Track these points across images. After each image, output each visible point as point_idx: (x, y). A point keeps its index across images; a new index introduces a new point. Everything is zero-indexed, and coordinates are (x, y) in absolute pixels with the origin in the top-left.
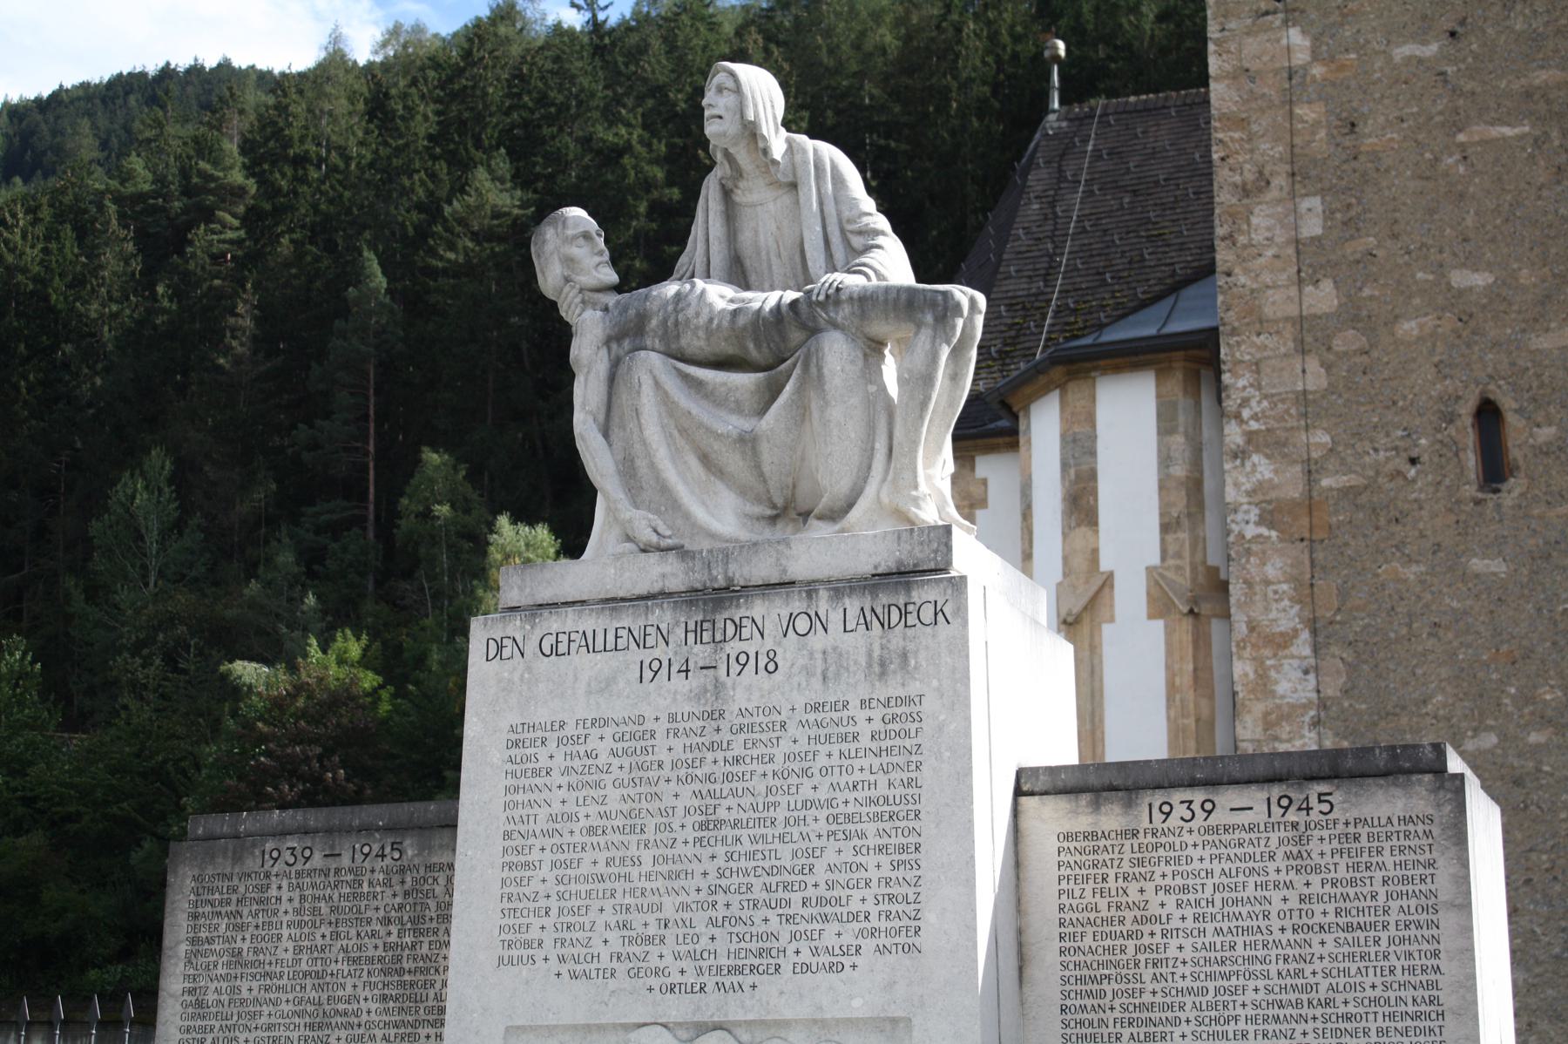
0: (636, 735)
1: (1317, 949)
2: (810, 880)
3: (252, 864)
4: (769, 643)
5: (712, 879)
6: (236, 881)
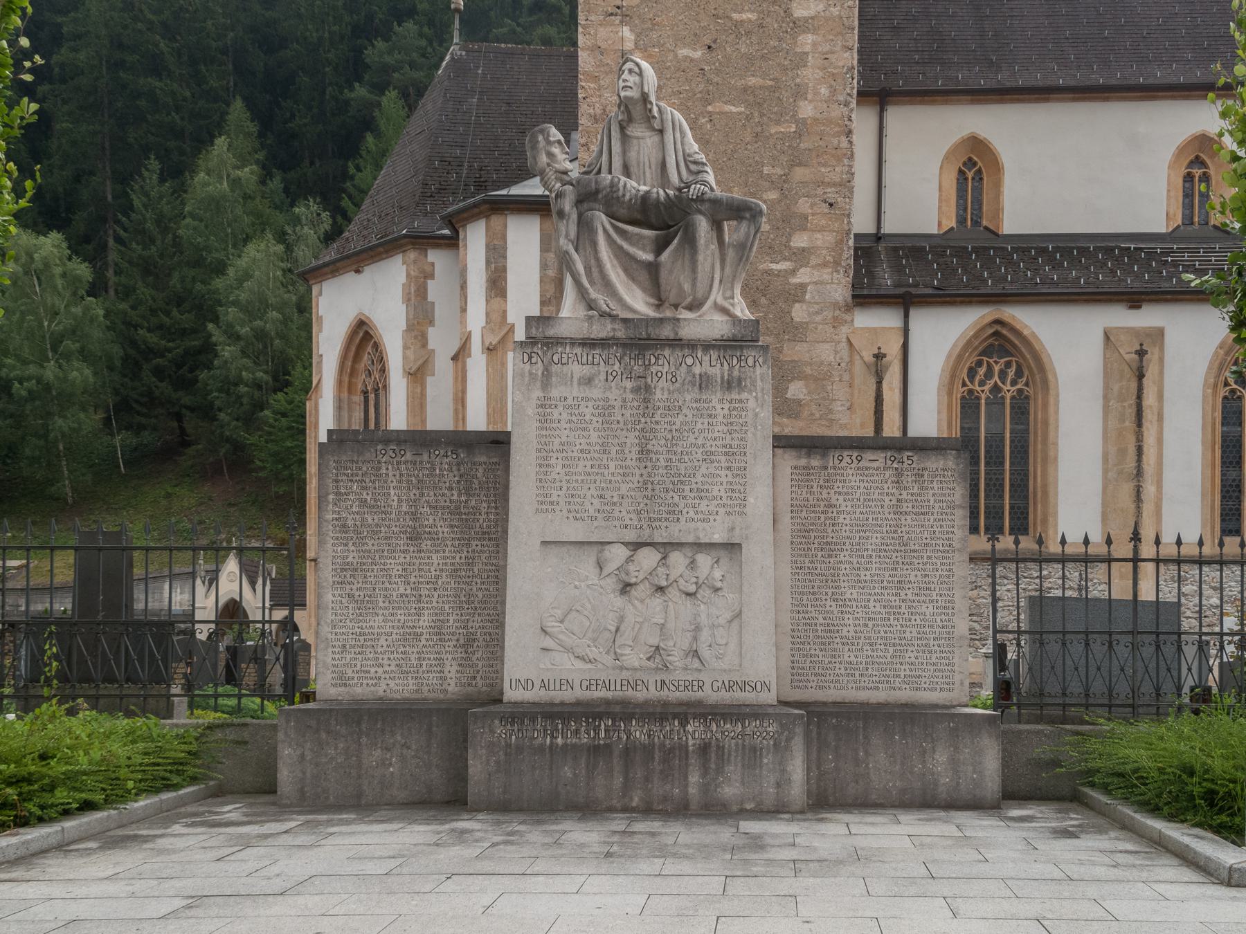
2: (694, 480)
3: (368, 456)
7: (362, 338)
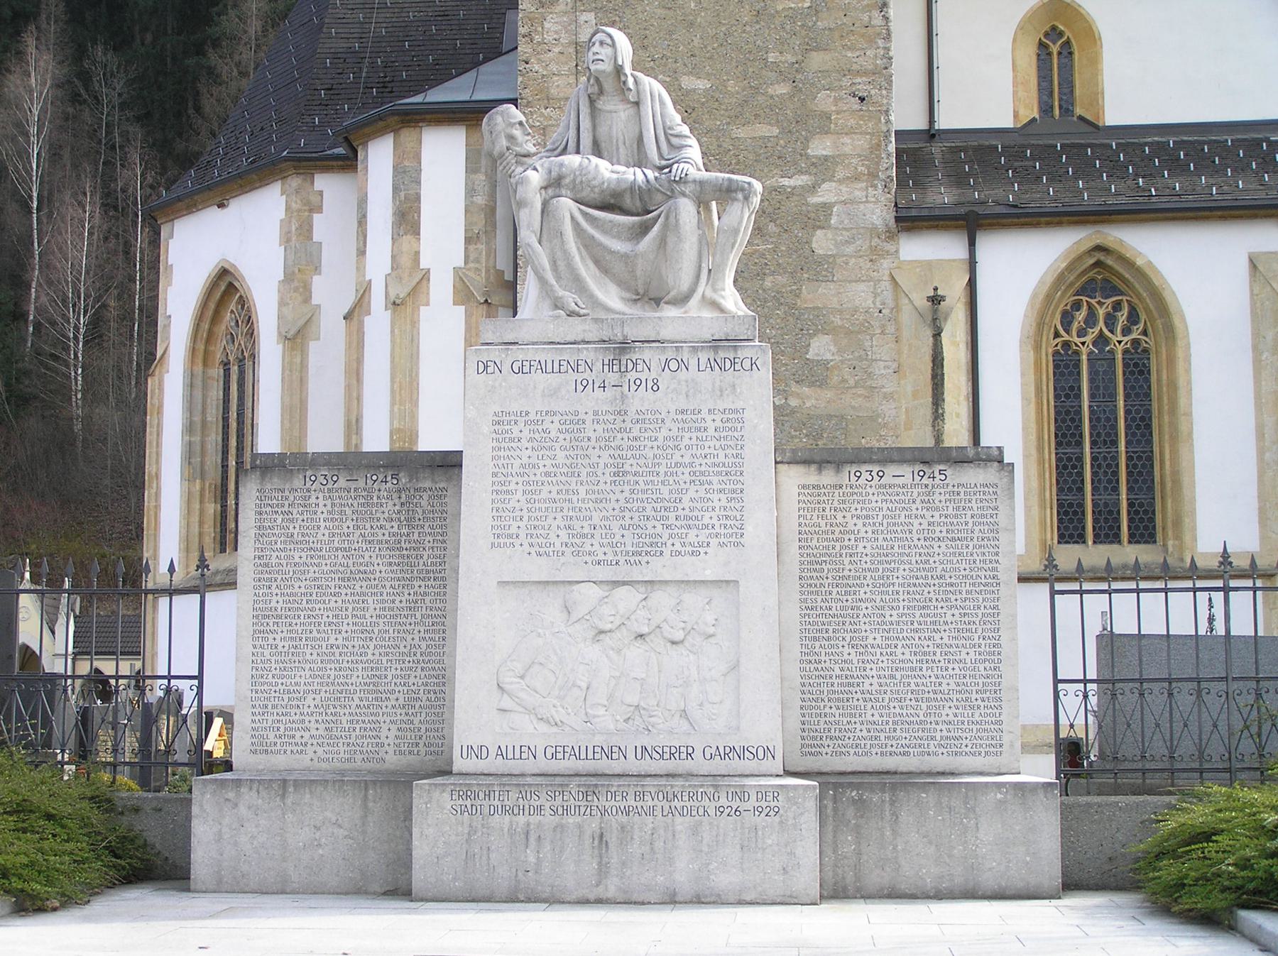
0: (573, 423)
1: (936, 550)
2: (680, 506)
4: (653, 375)
5: (622, 503)
6: (287, 493)
7: (225, 290)
